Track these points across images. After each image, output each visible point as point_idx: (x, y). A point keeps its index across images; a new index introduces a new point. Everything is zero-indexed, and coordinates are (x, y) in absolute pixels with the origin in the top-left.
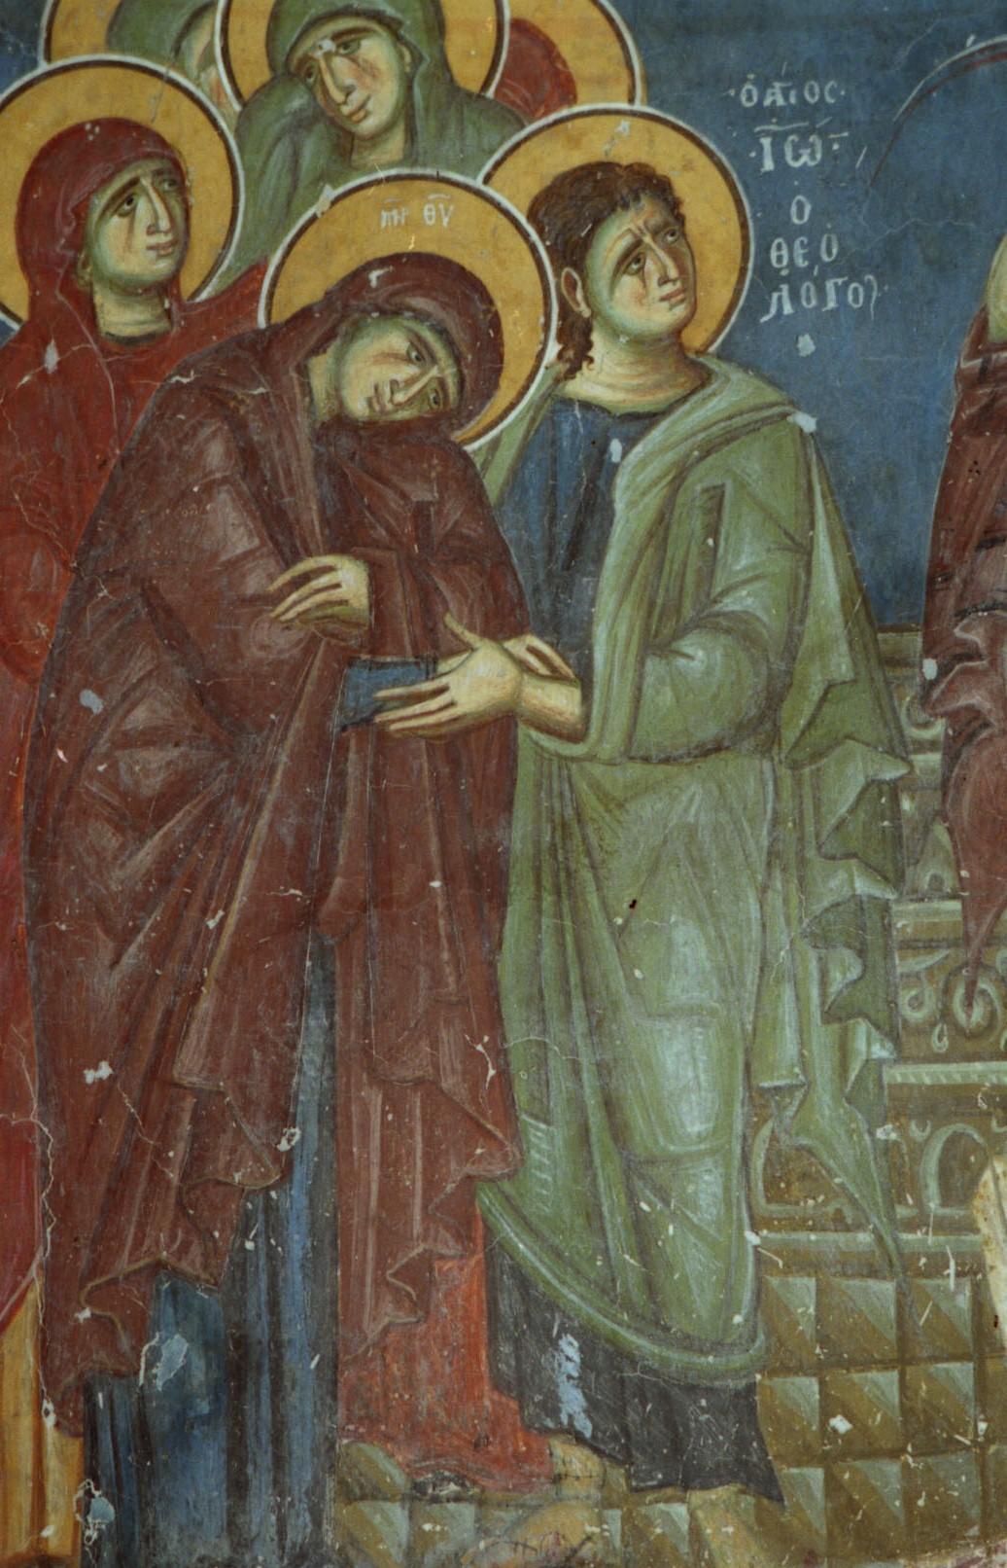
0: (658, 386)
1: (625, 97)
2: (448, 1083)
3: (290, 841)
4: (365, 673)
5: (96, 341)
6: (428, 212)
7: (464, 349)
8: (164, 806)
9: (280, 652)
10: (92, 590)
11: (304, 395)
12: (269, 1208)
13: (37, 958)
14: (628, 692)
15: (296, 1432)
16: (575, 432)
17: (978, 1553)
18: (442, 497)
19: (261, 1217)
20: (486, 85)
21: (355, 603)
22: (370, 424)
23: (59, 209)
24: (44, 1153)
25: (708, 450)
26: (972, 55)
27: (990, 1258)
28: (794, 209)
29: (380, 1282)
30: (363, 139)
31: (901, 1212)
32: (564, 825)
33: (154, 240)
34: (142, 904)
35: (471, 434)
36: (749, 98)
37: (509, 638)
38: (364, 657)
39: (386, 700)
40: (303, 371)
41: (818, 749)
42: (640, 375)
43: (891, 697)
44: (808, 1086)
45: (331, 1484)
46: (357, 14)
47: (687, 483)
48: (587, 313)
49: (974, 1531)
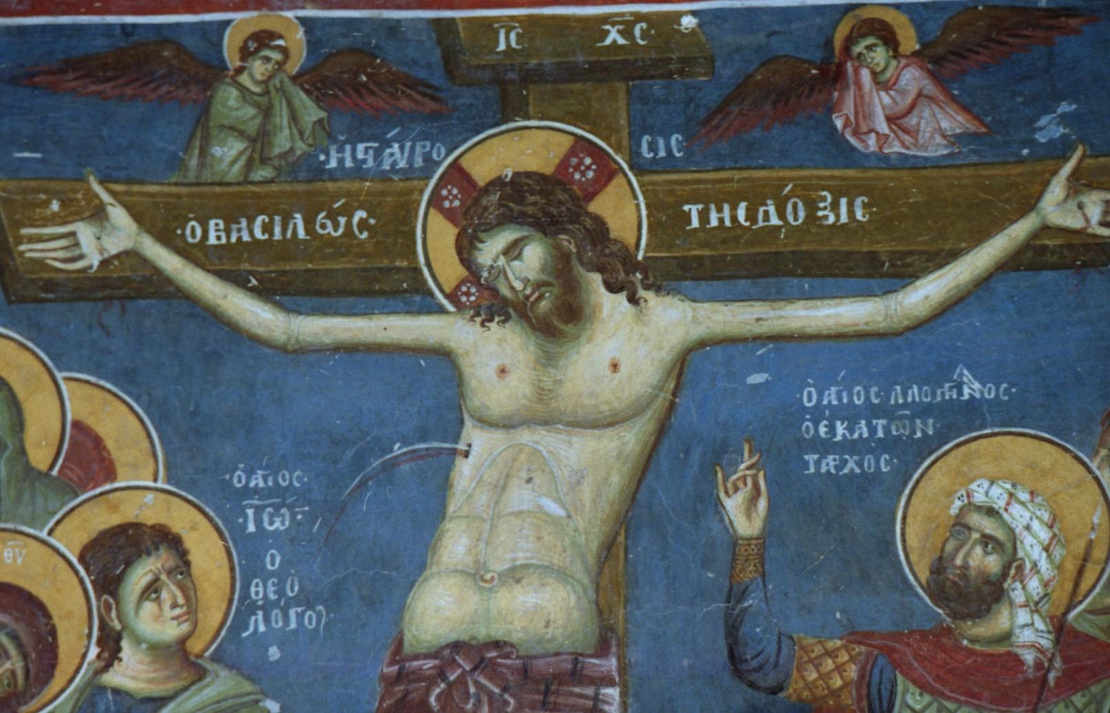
0: (168, 679)
1: (151, 478)
6: (7, 554)
7: (29, 649)
26: (397, 457)
28: (268, 559)
36: (240, 481)
42: (156, 671)
48: (118, 626)
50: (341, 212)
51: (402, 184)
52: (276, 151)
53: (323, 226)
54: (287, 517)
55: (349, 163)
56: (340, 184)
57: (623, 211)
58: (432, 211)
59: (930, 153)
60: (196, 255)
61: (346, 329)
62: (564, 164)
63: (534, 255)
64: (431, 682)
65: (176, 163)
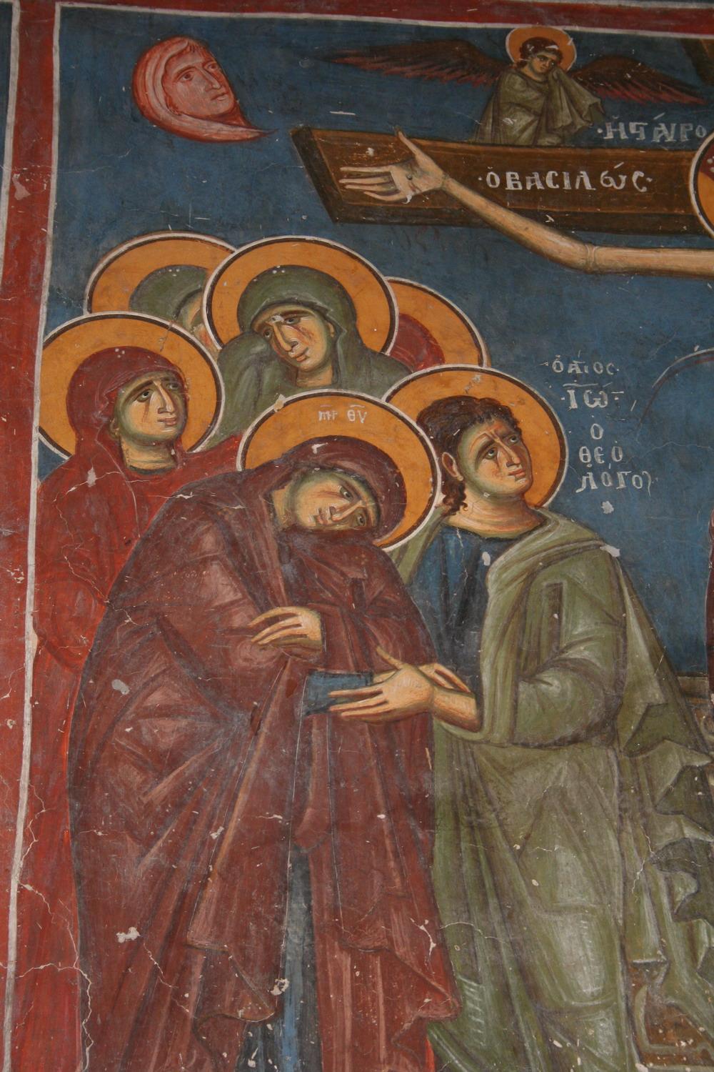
0: (509, 524)
2: (399, 952)
3: (272, 783)
4: (322, 679)
5: (123, 470)
6: (350, 415)
9: (258, 663)
10: (121, 617)
11: (270, 512)
12: (267, 1036)
13: (79, 854)
14: (508, 701)
16: (457, 546)
18: (369, 576)
19: (260, 1043)
21: (312, 638)
22: (317, 532)
23: (97, 394)
24: (84, 993)
25: (549, 562)
26: (698, 355)
28: (592, 431)
30: (304, 371)
32: (472, 784)
33: (163, 416)
34: (161, 821)
35: (387, 542)
36: (558, 368)
37: (422, 664)
38: (320, 670)
39: (337, 697)
40: (269, 498)
41: (640, 748)
42: (503, 516)
43: (693, 718)
44: (670, 962)
46: (298, 303)
47: (536, 580)
48: (461, 478)
50: (621, 171)
51: (672, 154)
52: (560, 125)
53: (607, 182)
54: (606, 397)
55: (623, 136)
56: (618, 151)
58: (701, 175)
60: (497, 196)
61: (637, 258)
65: (473, 128)
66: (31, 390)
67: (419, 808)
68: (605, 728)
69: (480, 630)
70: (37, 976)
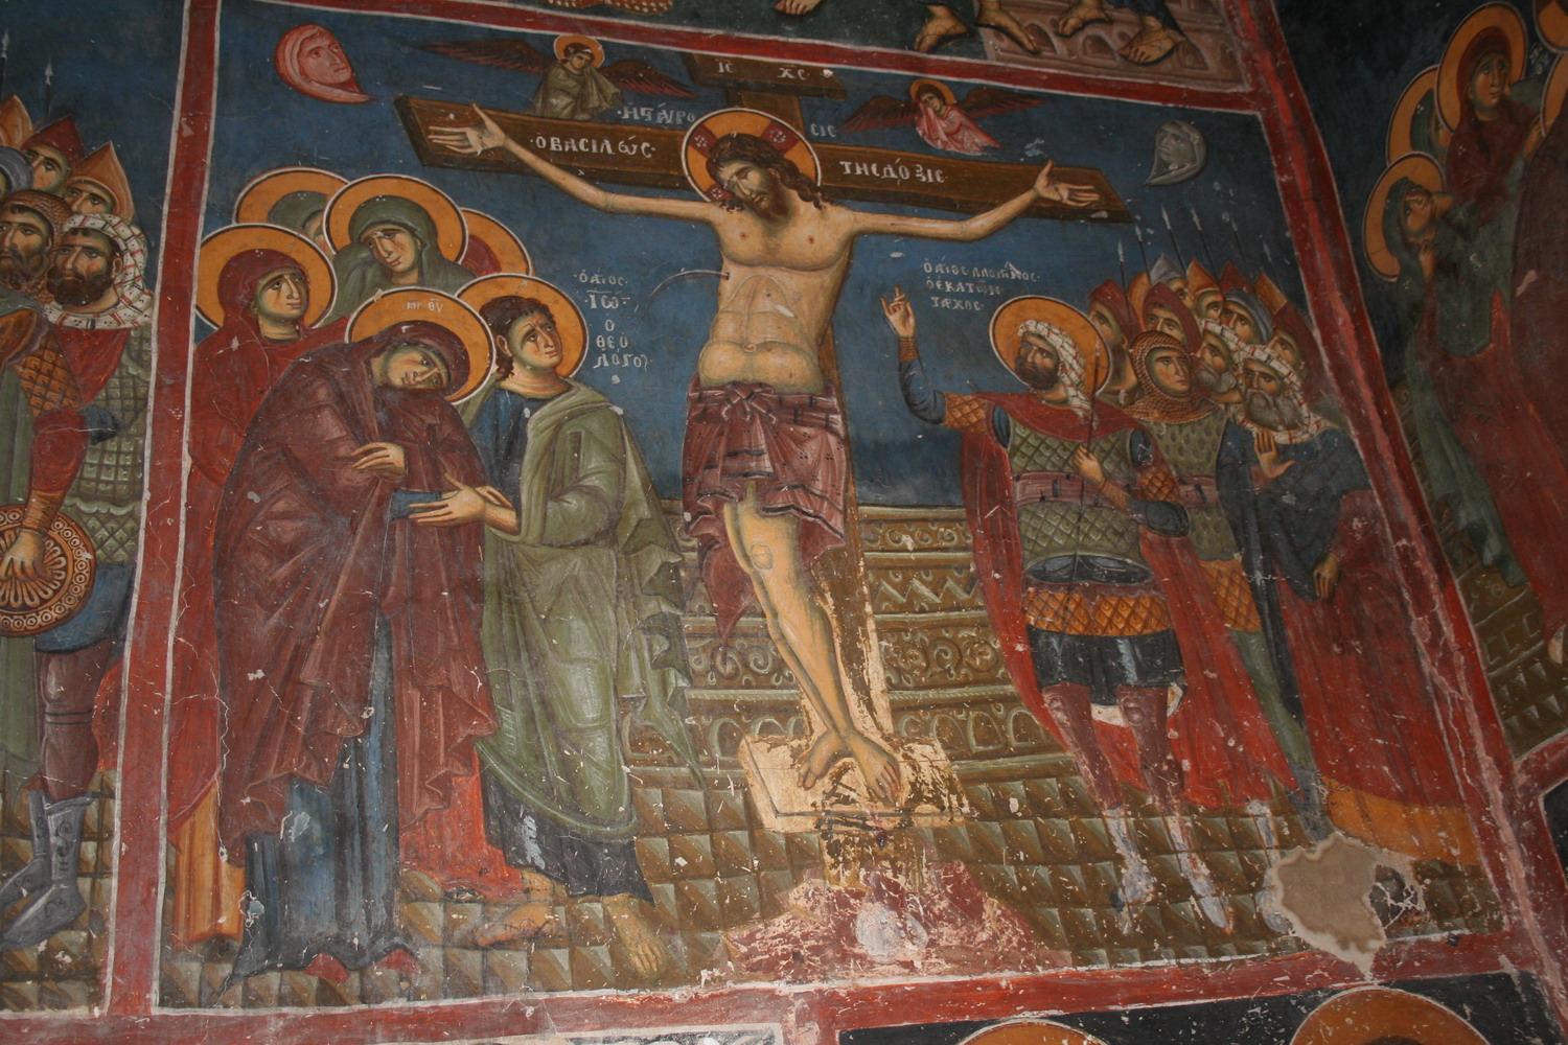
0: (545, 389)
2: (456, 689)
3: (365, 568)
6: (431, 306)
8: (291, 550)
10: (255, 447)
12: (358, 747)
14: (540, 515)
15: (376, 864)
17: (760, 926)
20: (458, 259)
22: (403, 389)
25: (572, 417)
27: (750, 781)
29: (422, 787)
31: (702, 758)
34: (282, 594)
40: (368, 363)
41: (633, 550)
44: (649, 697)
45: (397, 893)
49: (757, 915)
50: (634, 141)
57: (806, 160)
59: (971, 154)
60: (544, 154)
62: (766, 133)
63: (754, 180)
64: (721, 404)
66: (190, 277)
67: (473, 589)
68: (608, 535)
69: (521, 463)
70: (187, 702)
